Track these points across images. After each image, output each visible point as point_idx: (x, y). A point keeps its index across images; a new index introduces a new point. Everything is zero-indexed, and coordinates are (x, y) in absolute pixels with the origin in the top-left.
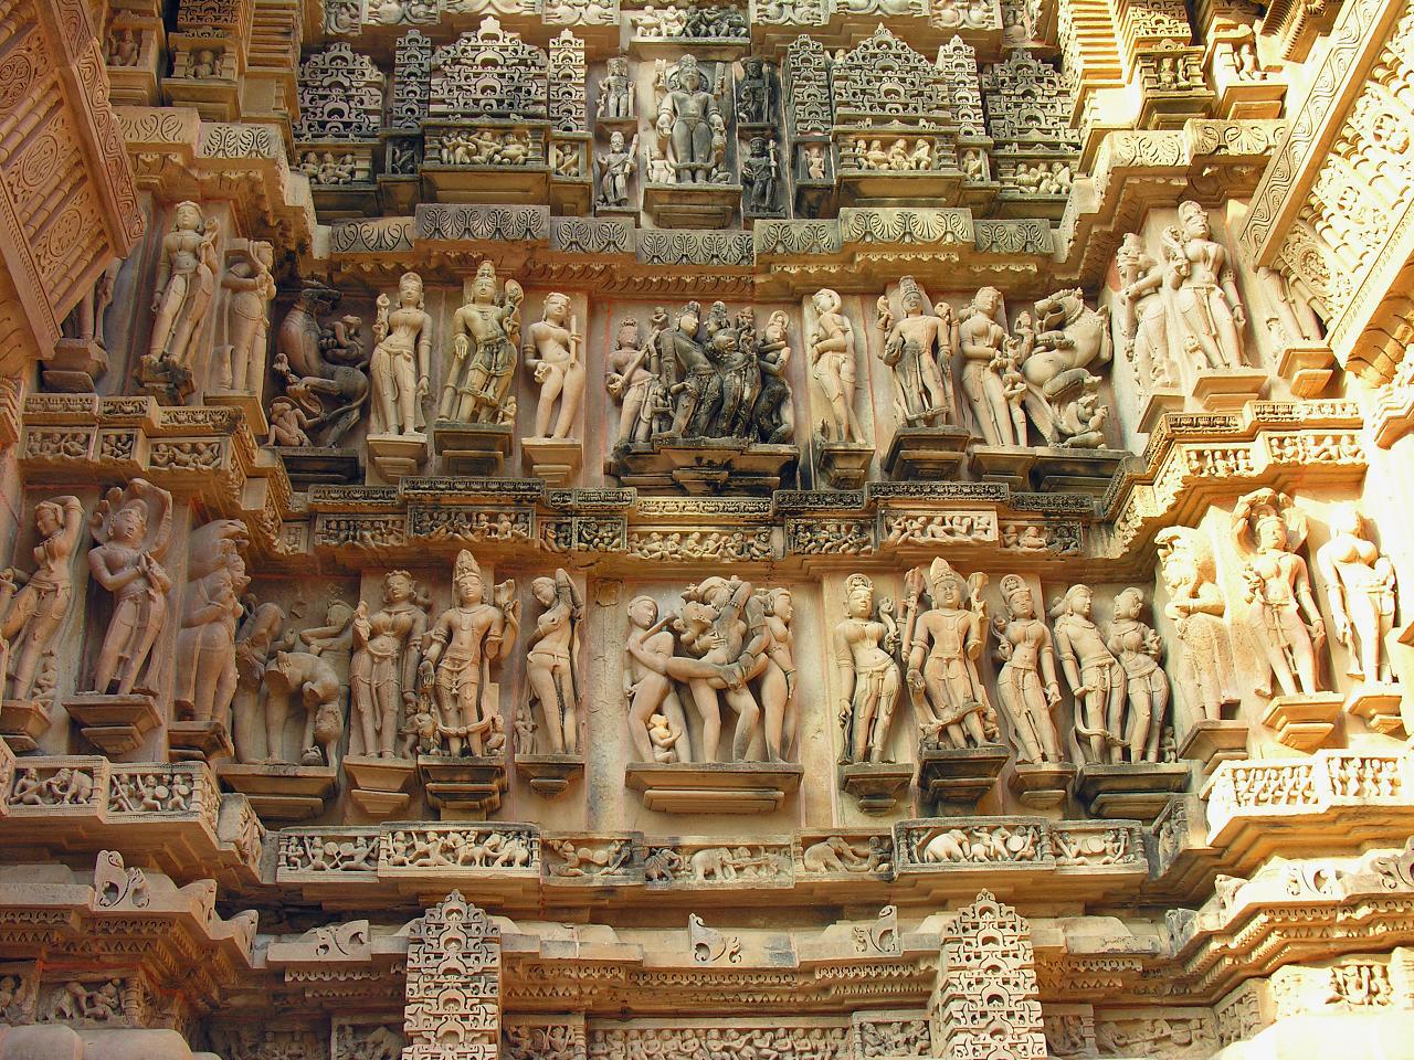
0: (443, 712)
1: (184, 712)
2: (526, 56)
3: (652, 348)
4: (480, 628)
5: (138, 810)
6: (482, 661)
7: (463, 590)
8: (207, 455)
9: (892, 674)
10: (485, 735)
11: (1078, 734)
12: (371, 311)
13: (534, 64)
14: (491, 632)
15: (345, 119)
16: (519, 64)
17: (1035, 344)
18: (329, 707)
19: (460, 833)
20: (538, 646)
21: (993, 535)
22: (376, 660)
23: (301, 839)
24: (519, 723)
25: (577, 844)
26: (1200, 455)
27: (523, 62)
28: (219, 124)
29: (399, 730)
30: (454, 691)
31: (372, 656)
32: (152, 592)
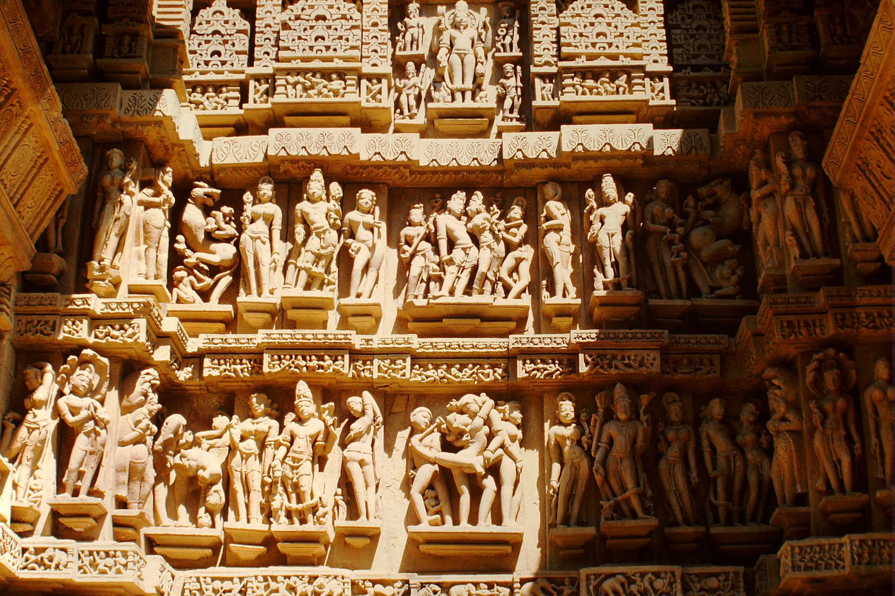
1: (122, 504)
2: (346, 12)
3: (432, 227)
4: (311, 437)
5: (96, 573)
8: (130, 331)
9: (585, 464)
10: (314, 509)
11: (710, 502)
12: (239, 208)
13: (351, 18)
15: (222, 58)
16: (341, 18)
17: (698, 218)
18: (214, 488)
19: (298, 577)
21: (656, 369)
23: (198, 579)
25: (374, 582)
27: (344, 17)
28: (135, 91)
30: (295, 480)
32: (98, 429)
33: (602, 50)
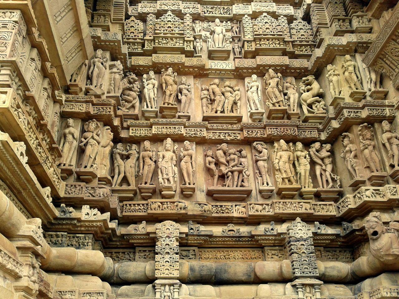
15: (135, 34)
26: (349, 112)
33: (268, 33)
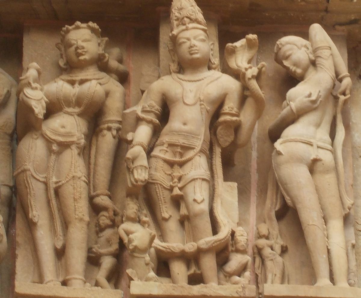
0: (158, 222)
4: (212, 102)
6: (211, 149)
7: (184, 49)
10: (222, 254)
14: (226, 108)
20: (290, 132)
22: (55, 147)
24: (262, 242)
29: (90, 250)
30: (176, 191)
31: (49, 142)
